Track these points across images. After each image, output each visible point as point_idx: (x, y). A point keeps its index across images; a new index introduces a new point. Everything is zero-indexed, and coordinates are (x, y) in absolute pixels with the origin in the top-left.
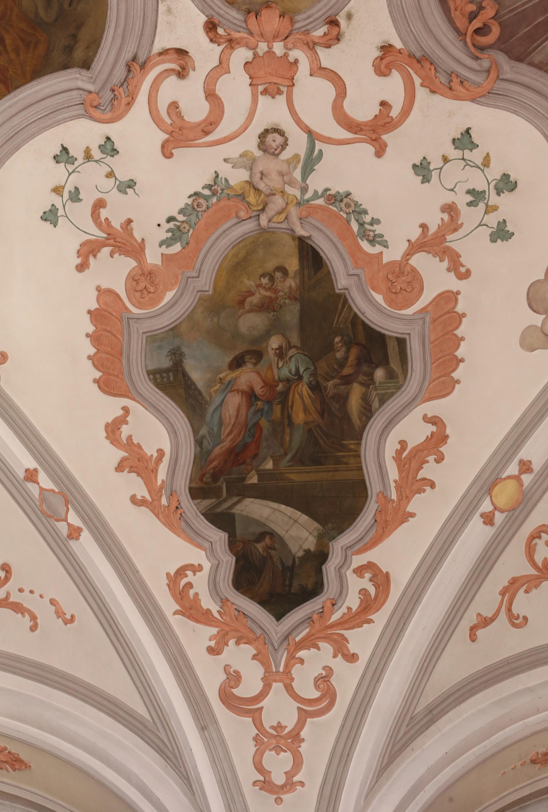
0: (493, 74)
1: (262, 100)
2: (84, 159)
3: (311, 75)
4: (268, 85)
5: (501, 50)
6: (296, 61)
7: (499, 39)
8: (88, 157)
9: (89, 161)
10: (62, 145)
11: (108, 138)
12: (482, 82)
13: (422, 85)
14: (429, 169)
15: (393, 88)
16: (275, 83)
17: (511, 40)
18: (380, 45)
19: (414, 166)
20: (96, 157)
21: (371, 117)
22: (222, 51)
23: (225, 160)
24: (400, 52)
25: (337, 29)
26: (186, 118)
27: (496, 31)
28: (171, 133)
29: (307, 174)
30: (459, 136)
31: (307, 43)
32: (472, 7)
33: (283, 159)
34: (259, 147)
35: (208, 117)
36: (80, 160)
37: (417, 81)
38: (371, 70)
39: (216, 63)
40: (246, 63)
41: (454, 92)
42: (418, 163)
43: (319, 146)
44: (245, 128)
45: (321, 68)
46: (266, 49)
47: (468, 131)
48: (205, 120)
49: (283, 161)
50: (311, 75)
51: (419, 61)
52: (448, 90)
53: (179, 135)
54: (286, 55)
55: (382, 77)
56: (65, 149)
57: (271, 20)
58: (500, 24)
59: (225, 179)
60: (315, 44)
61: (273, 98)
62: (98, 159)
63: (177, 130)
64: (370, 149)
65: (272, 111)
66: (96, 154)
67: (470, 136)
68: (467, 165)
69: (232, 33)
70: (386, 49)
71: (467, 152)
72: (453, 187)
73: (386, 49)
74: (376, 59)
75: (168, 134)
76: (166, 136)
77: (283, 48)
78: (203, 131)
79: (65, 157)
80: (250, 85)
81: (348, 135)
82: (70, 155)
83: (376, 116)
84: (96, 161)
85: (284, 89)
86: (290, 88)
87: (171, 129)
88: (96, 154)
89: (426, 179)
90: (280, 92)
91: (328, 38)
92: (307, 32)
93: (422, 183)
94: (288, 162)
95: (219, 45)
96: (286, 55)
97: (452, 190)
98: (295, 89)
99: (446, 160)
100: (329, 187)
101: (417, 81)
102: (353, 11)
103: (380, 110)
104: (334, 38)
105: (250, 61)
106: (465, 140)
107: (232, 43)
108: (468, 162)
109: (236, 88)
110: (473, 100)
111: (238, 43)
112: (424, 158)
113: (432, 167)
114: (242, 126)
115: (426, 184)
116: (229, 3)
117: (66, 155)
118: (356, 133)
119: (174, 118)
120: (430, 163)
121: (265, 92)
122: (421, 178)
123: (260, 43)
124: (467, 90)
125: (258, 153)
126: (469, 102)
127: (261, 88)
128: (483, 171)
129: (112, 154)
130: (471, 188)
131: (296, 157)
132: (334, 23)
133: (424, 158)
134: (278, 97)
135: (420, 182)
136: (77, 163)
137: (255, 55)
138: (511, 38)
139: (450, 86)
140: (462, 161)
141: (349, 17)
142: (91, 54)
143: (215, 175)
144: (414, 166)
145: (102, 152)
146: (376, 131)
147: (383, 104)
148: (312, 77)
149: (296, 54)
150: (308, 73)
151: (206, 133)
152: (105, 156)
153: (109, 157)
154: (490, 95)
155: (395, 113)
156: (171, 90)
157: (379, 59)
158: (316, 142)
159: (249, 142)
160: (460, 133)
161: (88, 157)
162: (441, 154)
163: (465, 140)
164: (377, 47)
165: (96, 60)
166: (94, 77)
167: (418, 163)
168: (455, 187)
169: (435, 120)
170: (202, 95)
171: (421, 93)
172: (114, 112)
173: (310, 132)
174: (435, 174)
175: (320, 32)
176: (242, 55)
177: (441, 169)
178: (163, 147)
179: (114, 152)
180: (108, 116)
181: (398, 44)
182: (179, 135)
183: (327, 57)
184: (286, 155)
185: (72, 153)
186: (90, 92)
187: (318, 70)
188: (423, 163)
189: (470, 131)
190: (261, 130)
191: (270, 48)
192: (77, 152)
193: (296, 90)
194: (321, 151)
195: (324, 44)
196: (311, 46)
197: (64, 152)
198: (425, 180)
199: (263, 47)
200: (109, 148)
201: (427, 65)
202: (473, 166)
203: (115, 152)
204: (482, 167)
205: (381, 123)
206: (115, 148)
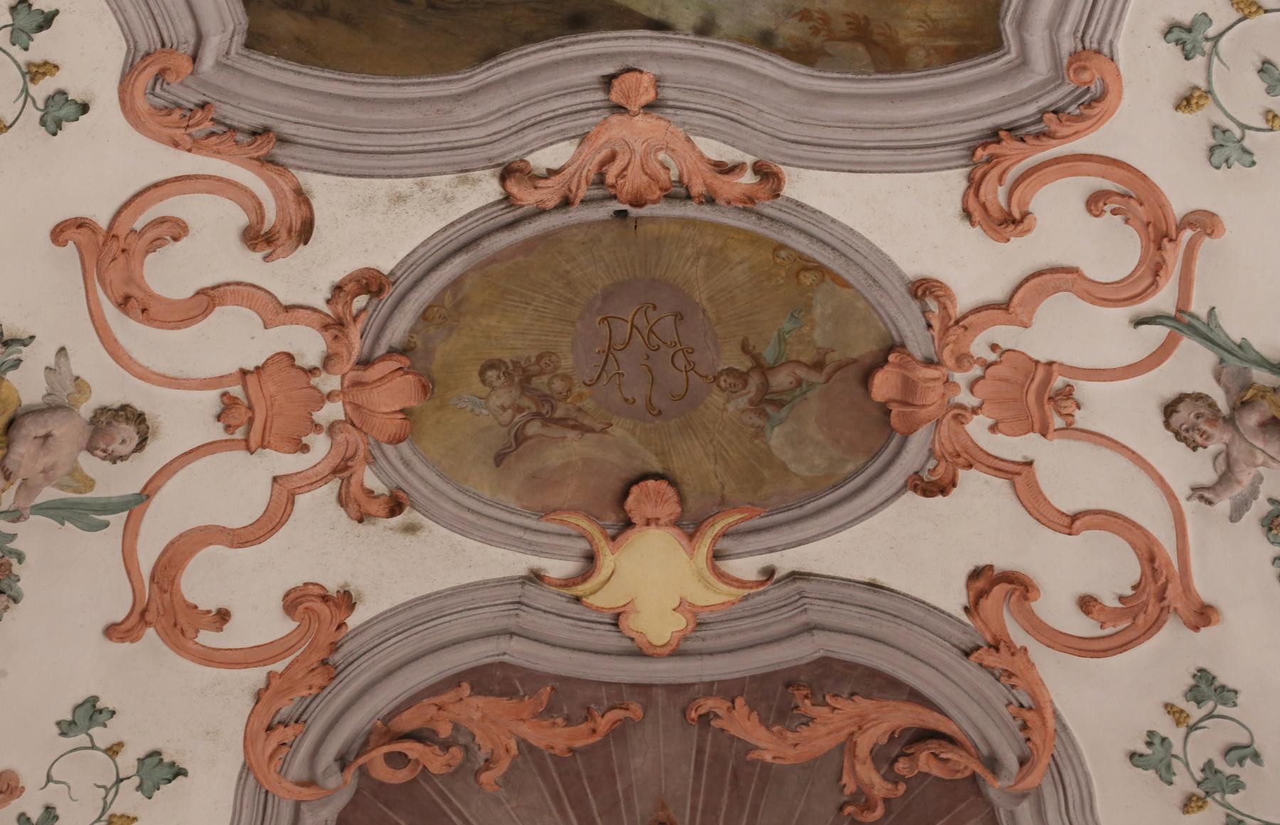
0: (305, 793)
1: (211, 399)
2: (29, 65)
3: (275, 479)
4: (246, 402)
5: (357, 792)
6: (305, 448)
7: (382, 784)
8: (36, 72)
9: (24, 75)
10: (56, 12)
11: (84, 108)
12: (290, 778)
13: (270, 675)
14: (89, 728)
15: (260, 623)
16: (251, 421)
17: (380, 805)
18: (352, 589)
19: (94, 700)
20: (32, 89)
21: (190, 598)
22: (315, 310)
23: (62, 350)
24: (341, 626)
25: (382, 513)
26: (151, 256)
27: (401, 776)
28: (111, 234)
29: (51, 512)
30: (167, 759)
31: (347, 468)
32: (445, 731)
33: (80, 459)
34: (104, 410)
35: (159, 299)
36: (22, 56)
37: (279, 667)
38: (296, 581)
39: (286, 299)
40: (290, 357)
41: (263, 735)
42: (99, 705)
43: (117, 520)
44: (146, 375)
45: (293, 495)
46: (326, 389)
47: (181, 772)
48: (151, 295)
49: (76, 461)
50: (275, 479)
51: (324, 662)
52: (266, 723)
53: (109, 251)
54: (317, 427)
55: (281, 603)
56: (47, 20)
57: (393, 393)
58: (414, 781)
59: (20, 361)
60: (346, 482)
61: (219, 418)
62: (31, 92)
63: (122, 246)
64: (120, 609)
65: (184, 420)
66: (41, 90)
67: (170, 781)
68: (108, 790)
69: (360, 326)
70: (347, 600)
71: (136, 781)
72: (55, 778)
73: (347, 600)
74: (322, 587)
75: (111, 227)
76: (103, 222)
77: (332, 419)
78: (127, 298)
79: (25, 20)
80: (244, 373)
81: (146, 568)
82: (33, 35)
83: (196, 607)
84: (25, 90)
85: (239, 434)
86: (243, 444)
87: (121, 230)
88: (41, 90)
89: (66, 728)
90: (228, 428)
91: (363, 499)
92: (371, 460)
93: (59, 724)
94: (75, 471)
95: (328, 301)
96: (317, 427)
97: (49, 779)
98: (241, 455)
99: (113, 751)
100: (28, 560)
101: (279, 667)
102: (422, 535)
103: (209, 612)
104: (358, 508)
105: (298, 363)
106: (160, 771)
107: (335, 326)
108: (114, 790)
109: (234, 341)
110: (247, 768)
111: (336, 337)
112: (113, 713)
113: (95, 731)
114: (147, 369)
115: (56, 730)
116: (425, 312)
117: (34, 25)
118: (152, 578)
119: (150, 235)
120: (105, 726)
121: (229, 404)
122: (69, 718)
123: (339, 377)
124: (271, 757)
125: (86, 410)
126: (242, 759)
127: (236, 390)
128: (98, 820)
129: (49, 119)
130: (59, 812)
131: (90, 484)
132: (395, 506)
133: (113, 713)
134: (221, 425)
135: (60, 718)
136: (16, 51)
137: (312, 371)
138: (385, 804)
139: (272, 724)
140: (114, 779)
141: (411, 529)
142: (285, 48)
143: (25, 336)
144: (94, 700)
145: (49, 99)
146: (161, 611)
147: (223, 616)
148: (270, 481)
149: (320, 445)
150: (278, 473)
151: (124, 303)
152: (41, 106)
153: (39, 114)
154: (263, 796)
155: (207, 638)
156: (214, 228)
157: (322, 592)
158: (125, 514)
159: (108, 386)
160: (174, 759)
161: (36, 72)
162: (123, 739)
163: (160, 771)
164: (346, 584)
165: (271, 59)
166: (229, 62)
167: (99, 705)
168: (57, 782)
169: (201, 713)
170: (208, 282)
171: (256, 676)
172: (151, 115)
173: (145, 496)
174: (82, 739)
175: (371, 480)
176: (308, 345)
177: (93, 747)
178: (81, 223)
179: (52, 124)
180: (142, 104)
181: (353, 621)
182: (109, 251)
183: (318, 503)
184: (90, 464)
185: (40, 37)
186: (194, 58)
187: (285, 495)
188: (104, 714)
189: (180, 778)
190: (139, 405)
191: (330, 396)
192: (43, 46)
193: (240, 455)
194: (107, 525)
195: (347, 493)
196: (342, 469)
197: (40, 19)
198: (64, 726)
199: (330, 382)
200: (63, 111)
201: (318, 680)
202: (105, 803)
203: (53, 127)
204: (105, 817)
205: (182, 620)
206: (64, 123)
